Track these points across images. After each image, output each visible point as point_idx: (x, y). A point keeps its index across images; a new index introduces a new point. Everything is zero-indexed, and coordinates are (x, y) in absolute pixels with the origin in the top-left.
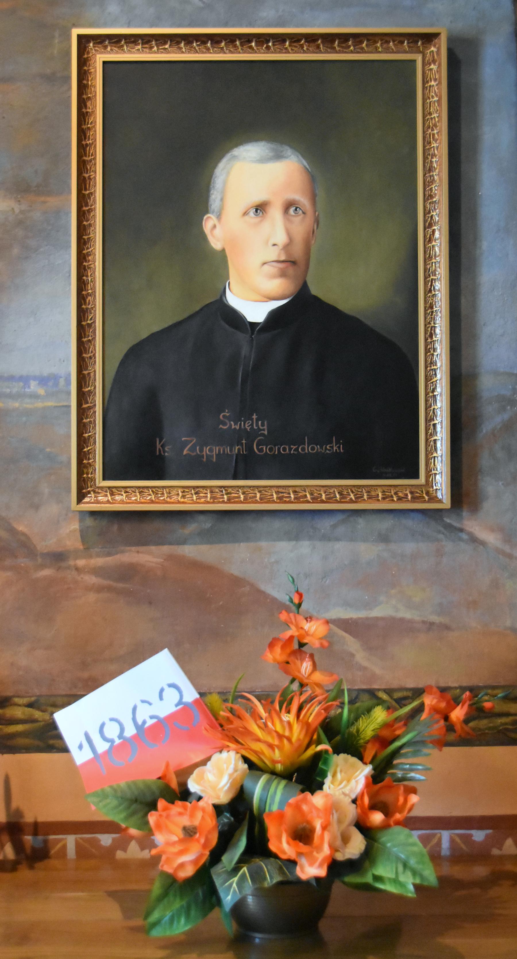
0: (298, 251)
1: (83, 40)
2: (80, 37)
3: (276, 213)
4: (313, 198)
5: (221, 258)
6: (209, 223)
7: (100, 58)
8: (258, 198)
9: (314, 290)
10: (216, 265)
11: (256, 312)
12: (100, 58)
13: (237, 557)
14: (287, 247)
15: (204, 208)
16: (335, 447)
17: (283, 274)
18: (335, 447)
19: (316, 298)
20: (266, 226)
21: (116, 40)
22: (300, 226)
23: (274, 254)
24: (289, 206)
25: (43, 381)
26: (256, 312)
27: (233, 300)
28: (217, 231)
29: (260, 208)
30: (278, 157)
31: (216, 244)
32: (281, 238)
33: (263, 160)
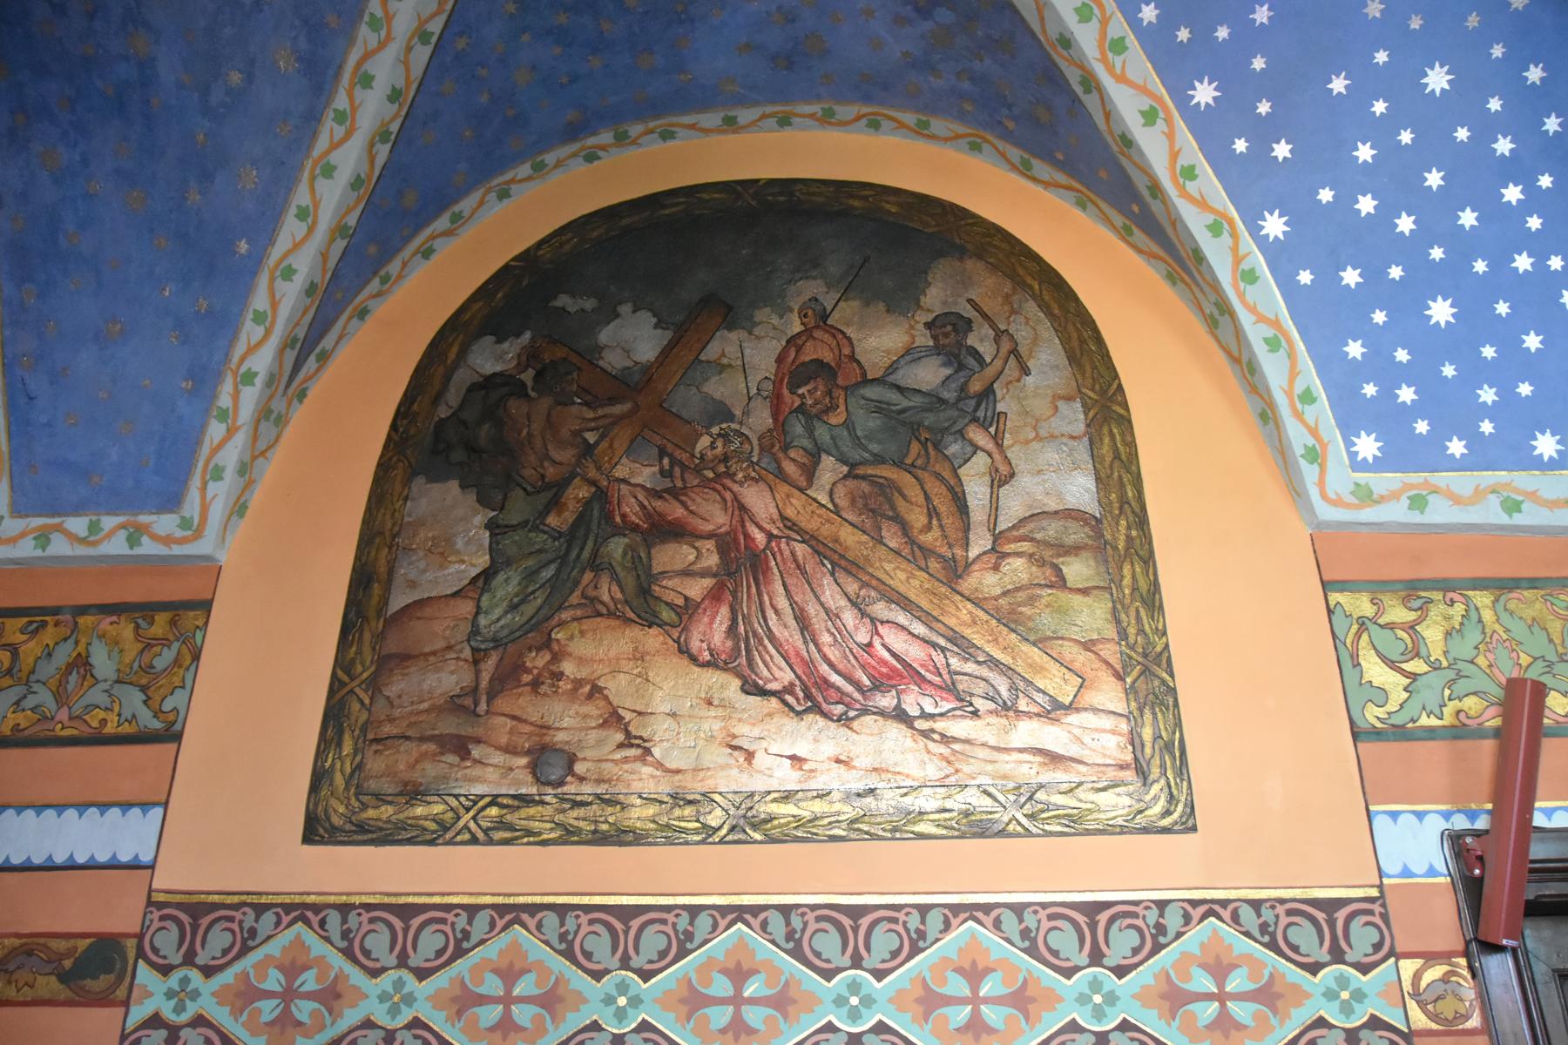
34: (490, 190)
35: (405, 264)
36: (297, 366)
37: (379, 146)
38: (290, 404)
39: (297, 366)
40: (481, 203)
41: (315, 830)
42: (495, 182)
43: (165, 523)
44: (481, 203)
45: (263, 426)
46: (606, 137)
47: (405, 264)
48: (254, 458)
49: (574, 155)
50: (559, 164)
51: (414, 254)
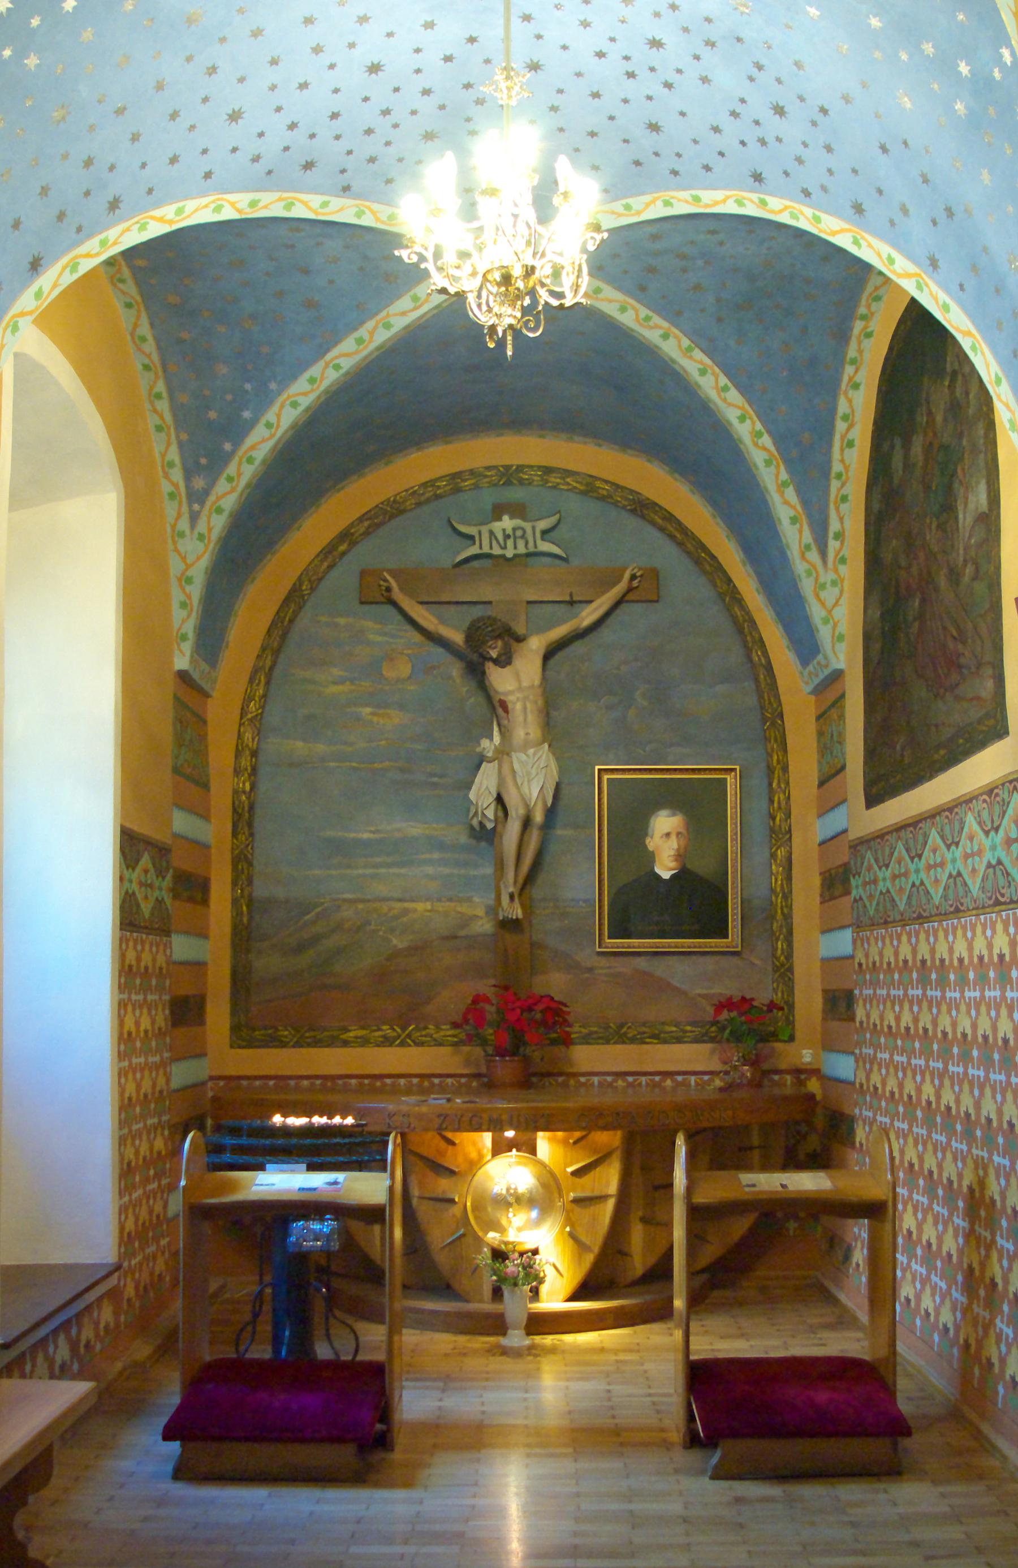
0: (682, 851)
1: (599, 770)
2: (599, 770)
3: (674, 837)
4: (687, 829)
5: (653, 853)
6: (648, 840)
7: (606, 777)
8: (666, 831)
9: (689, 866)
10: (650, 858)
11: (666, 875)
12: (606, 777)
13: (660, 968)
14: (678, 850)
15: (646, 835)
16: (696, 927)
17: (676, 860)
18: (696, 927)
19: (688, 870)
20: (670, 842)
21: (612, 771)
22: (683, 842)
23: (672, 853)
24: (678, 834)
25: (585, 901)
26: (666, 875)
27: (657, 870)
28: (651, 844)
29: (668, 835)
30: (674, 815)
31: (651, 849)
32: (675, 846)
33: (669, 816)
34: (846, 393)
35: (842, 461)
36: (823, 554)
37: (760, 442)
38: (836, 571)
39: (823, 554)
40: (850, 401)
41: (872, 800)
42: (843, 386)
43: (820, 657)
44: (850, 401)
45: (823, 595)
46: (858, 326)
47: (842, 461)
48: (830, 612)
49: (860, 343)
50: (860, 351)
51: (842, 450)
